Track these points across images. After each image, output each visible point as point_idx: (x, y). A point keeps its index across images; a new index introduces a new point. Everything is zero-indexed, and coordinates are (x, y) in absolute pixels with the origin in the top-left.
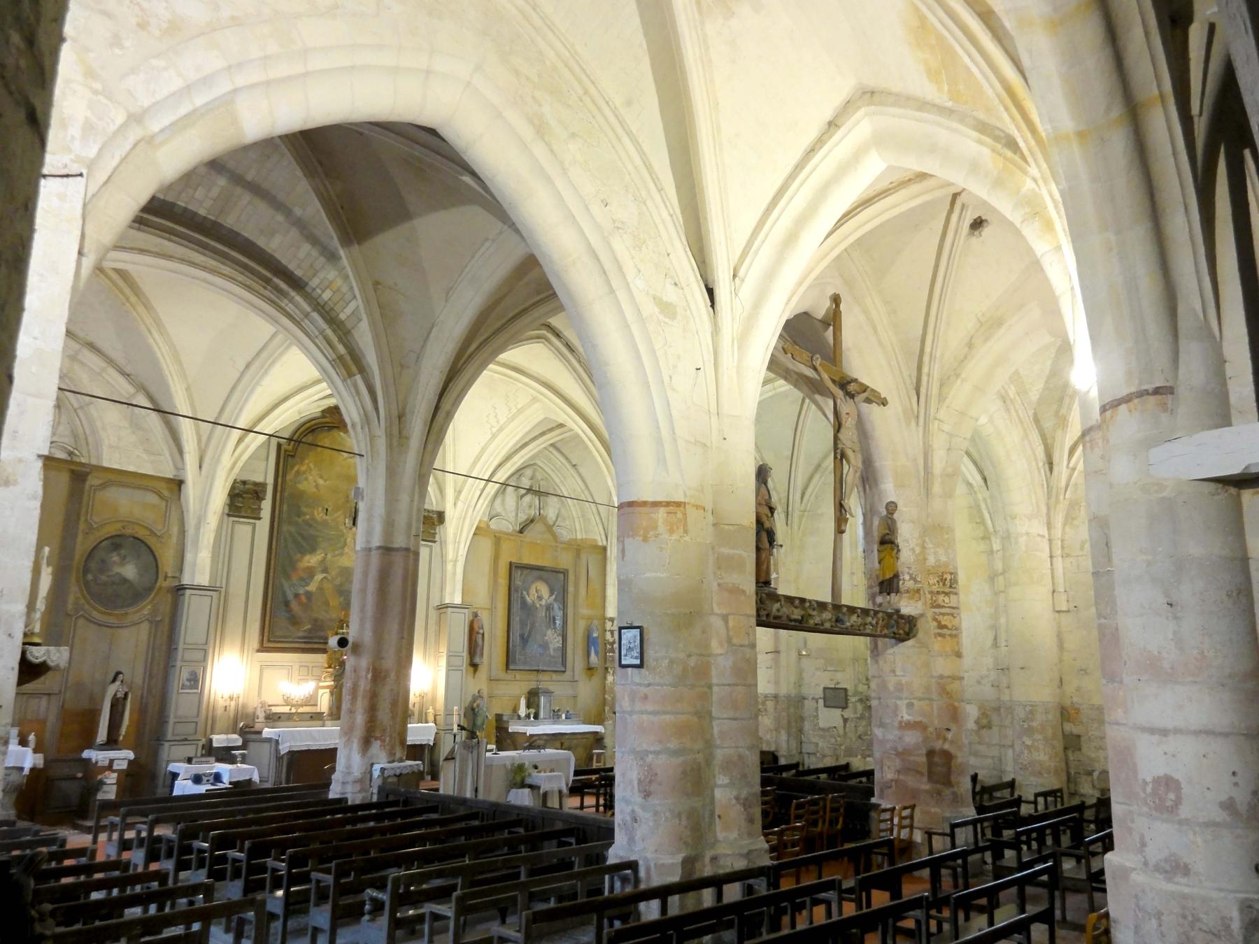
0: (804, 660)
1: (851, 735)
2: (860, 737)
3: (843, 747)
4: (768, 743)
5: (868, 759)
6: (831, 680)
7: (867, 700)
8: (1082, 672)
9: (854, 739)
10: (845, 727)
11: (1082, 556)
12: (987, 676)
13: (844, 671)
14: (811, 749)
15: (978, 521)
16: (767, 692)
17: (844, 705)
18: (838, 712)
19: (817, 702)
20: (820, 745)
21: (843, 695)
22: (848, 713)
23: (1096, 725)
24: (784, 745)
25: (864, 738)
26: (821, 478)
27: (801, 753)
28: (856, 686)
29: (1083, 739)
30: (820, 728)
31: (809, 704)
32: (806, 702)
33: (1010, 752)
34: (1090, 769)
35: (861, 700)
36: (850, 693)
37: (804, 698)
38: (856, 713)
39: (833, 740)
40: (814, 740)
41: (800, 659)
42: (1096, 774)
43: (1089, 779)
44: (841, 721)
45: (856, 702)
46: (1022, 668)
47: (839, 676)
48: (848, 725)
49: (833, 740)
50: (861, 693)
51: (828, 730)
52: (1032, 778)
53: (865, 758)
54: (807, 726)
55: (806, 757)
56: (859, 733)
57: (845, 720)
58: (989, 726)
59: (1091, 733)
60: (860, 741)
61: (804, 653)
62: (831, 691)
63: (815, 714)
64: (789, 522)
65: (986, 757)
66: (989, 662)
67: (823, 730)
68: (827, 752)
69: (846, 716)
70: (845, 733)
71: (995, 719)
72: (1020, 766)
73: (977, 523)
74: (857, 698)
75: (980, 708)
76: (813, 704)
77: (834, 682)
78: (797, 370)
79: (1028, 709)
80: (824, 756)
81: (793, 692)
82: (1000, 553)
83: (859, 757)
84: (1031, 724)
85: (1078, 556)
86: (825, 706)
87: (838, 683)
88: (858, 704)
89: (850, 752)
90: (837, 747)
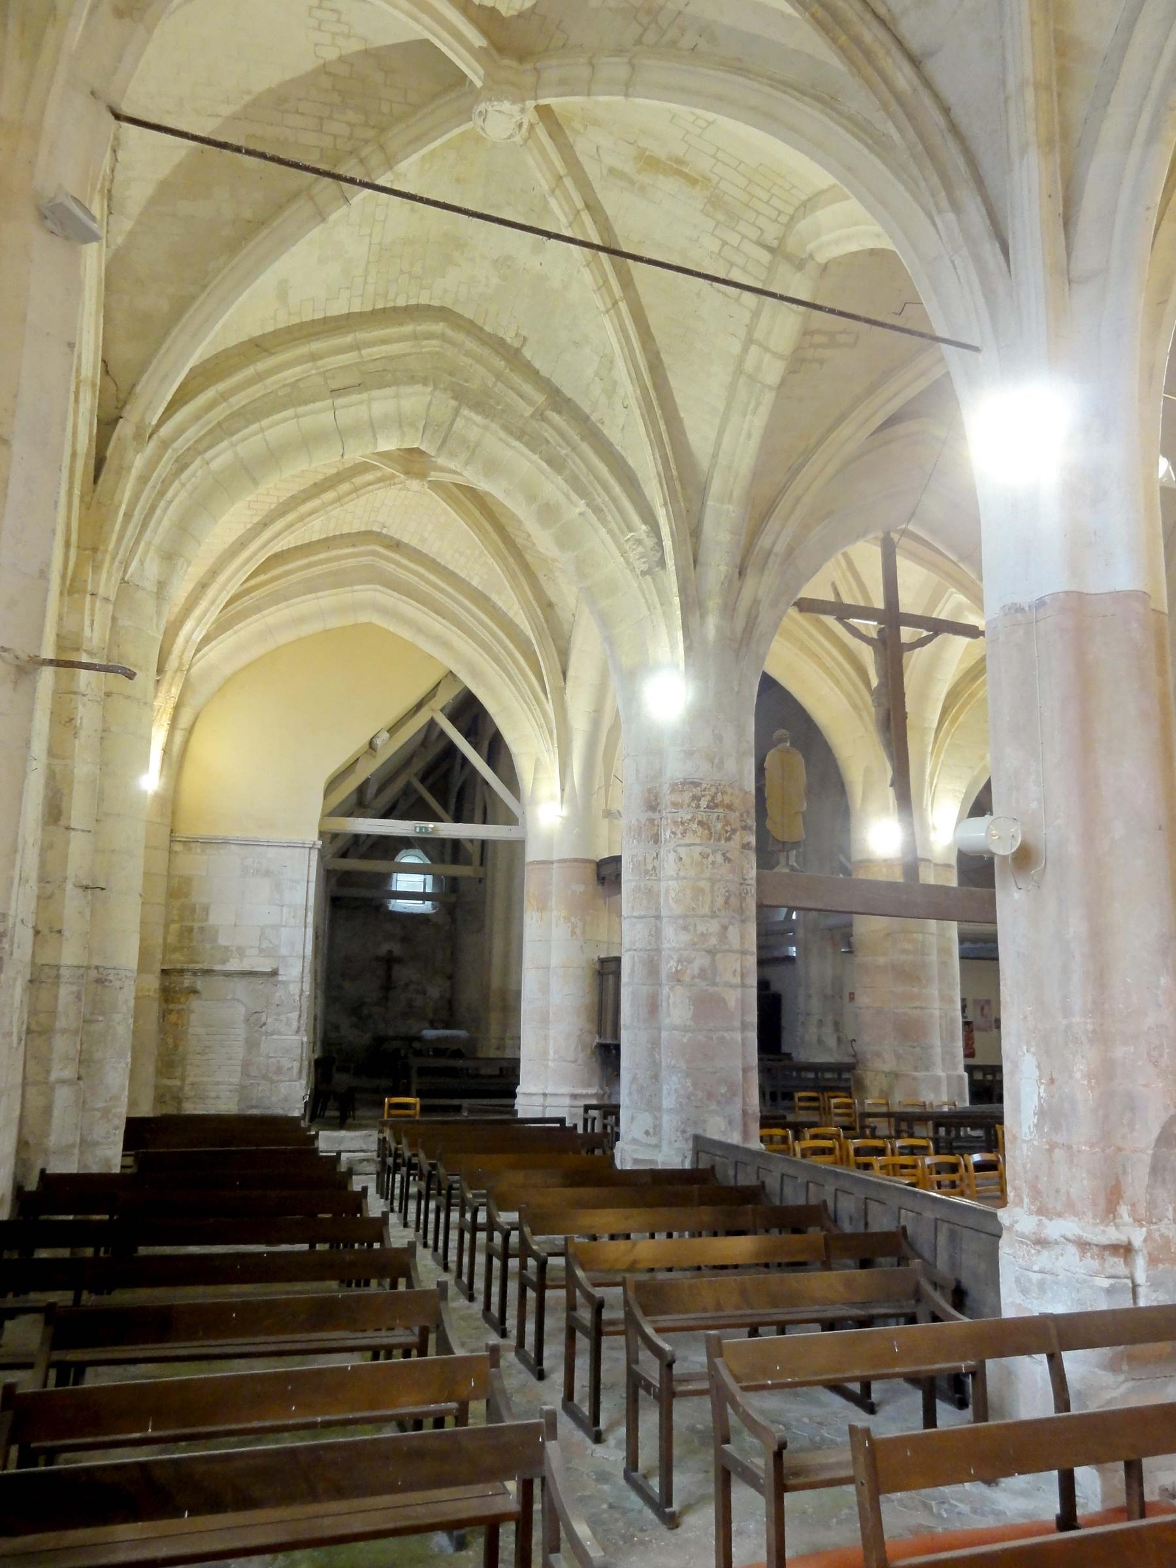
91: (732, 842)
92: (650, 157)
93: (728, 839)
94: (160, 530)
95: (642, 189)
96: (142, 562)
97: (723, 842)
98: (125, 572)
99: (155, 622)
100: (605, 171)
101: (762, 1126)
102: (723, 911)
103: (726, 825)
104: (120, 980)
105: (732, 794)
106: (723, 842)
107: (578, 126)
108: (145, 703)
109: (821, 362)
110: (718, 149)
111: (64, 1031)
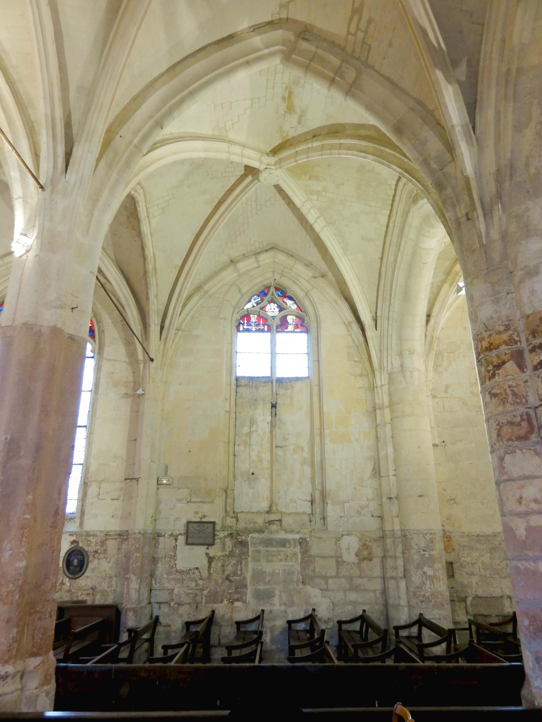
0: (162, 490)
1: (217, 577)
2: (227, 578)
3: (205, 593)
4: (104, 593)
5: (237, 604)
6: (197, 513)
7: (238, 534)
8: (452, 502)
9: (220, 581)
10: (210, 567)
11: (447, 398)
12: (367, 506)
13: (212, 502)
14: (161, 596)
15: (356, 360)
16: (108, 529)
17: (211, 541)
18: (201, 550)
19: (176, 540)
20: (176, 592)
21: (210, 529)
22: (213, 551)
23: (466, 552)
24: (134, 595)
25: (231, 578)
26: (200, 299)
27: (150, 603)
28: (224, 519)
29: (455, 566)
30: (177, 571)
31: (165, 543)
32: (161, 539)
33: (403, 584)
34: (463, 595)
35: (231, 535)
36: (218, 528)
37: (159, 535)
38: (223, 549)
39: (193, 584)
40: (167, 585)
41: (158, 489)
42: (469, 600)
43: (463, 605)
44: (205, 561)
45: (225, 537)
46: (420, 496)
47: (206, 508)
48: (213, 564)
49: (193, 584)
50: (231, 527)
51: (188, 572)
52: (435, 612)
53: (232, 603)
54: (160, 568)
55: (156, 606)
56: (227, 573)
57: (211, 560)
58: (370, 558)
59: (462, 559)
60: (227, 583)
61: (165, 482)
62: (195, 525)
63: (173, 554)
64: (163, 336)
65: (366, 590)
66: (368, 492)
67: (181, 572)
68: (185, 599)
69: (211, 555)
70: (210, 573)
71: (377, 551)
72: (421, 598)
73: (355, 361)
74: (226, 533)
75: (360, 539)
76: (171, 542)
77: (200, 515)
78: (421, 22)
79: (428, 537)
80: (180, 604)
81: (150, 529)
82: (385, 388)
83: (225, 602)
84: (431, 553)
85: (443, 398)
86: (187, 543)
87: (204, 516)
88: (228, 540)
89: (214, 597)
90: (198, 592)
91: (497, 377)
92: (287, 109)
93: (494, 375)
94: (393, 346)
95: (303, 111)
96: (392, 363)
97: (487, 382)
98: (388, 371)
99: (403, 381)
100: (300, 126)
101: (522, 668)
102: (497, 444)
103: (488, 366)
104: (411, 534)
105: (490, 335)
106: (487, 382)
107: (285, 135)
108: (404, 416)
109: (370, 21)
110: (267, 88)
111: (391, 557)
